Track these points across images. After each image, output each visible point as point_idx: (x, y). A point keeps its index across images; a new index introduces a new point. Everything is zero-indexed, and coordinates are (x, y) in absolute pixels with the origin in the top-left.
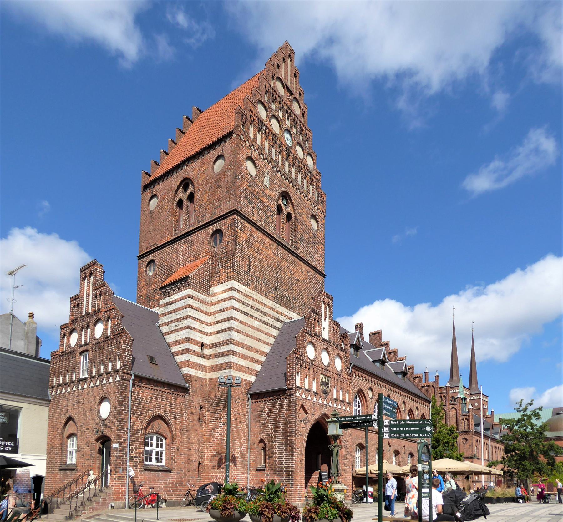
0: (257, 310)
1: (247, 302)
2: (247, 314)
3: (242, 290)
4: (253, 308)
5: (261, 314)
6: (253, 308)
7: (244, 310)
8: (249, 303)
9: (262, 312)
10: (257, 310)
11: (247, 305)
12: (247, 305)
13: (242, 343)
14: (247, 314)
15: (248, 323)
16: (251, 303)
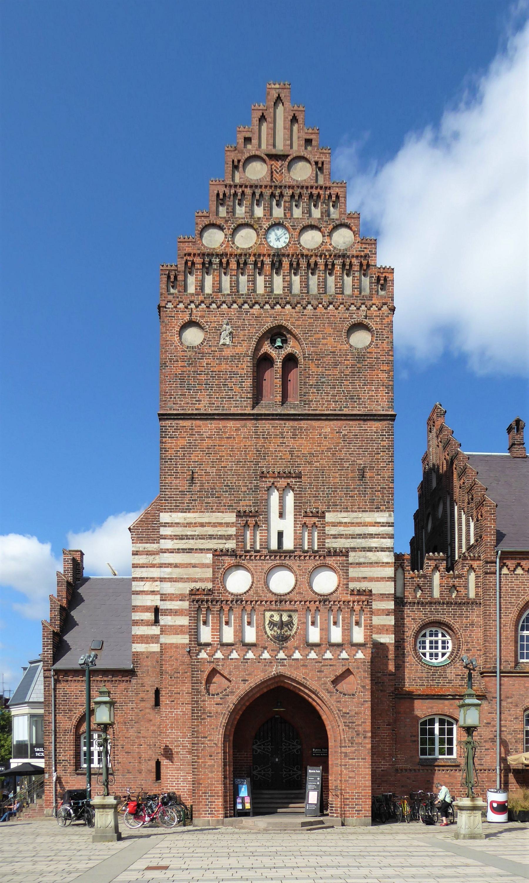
0: (211, 537)
1: (189, 533)
2: (190, 551)
3: (177, 521)
4: (202, 537)
5: (220, 541)
6: (202, 537)
7: (184, 547)
8: (193, 533)
9: (221, 537)
10: (211, 537)
11: (188, 537)
12: (188, 537)
13: (180, 594)
14: (190, 551)
15: (193, 562)
16: (199, 531)
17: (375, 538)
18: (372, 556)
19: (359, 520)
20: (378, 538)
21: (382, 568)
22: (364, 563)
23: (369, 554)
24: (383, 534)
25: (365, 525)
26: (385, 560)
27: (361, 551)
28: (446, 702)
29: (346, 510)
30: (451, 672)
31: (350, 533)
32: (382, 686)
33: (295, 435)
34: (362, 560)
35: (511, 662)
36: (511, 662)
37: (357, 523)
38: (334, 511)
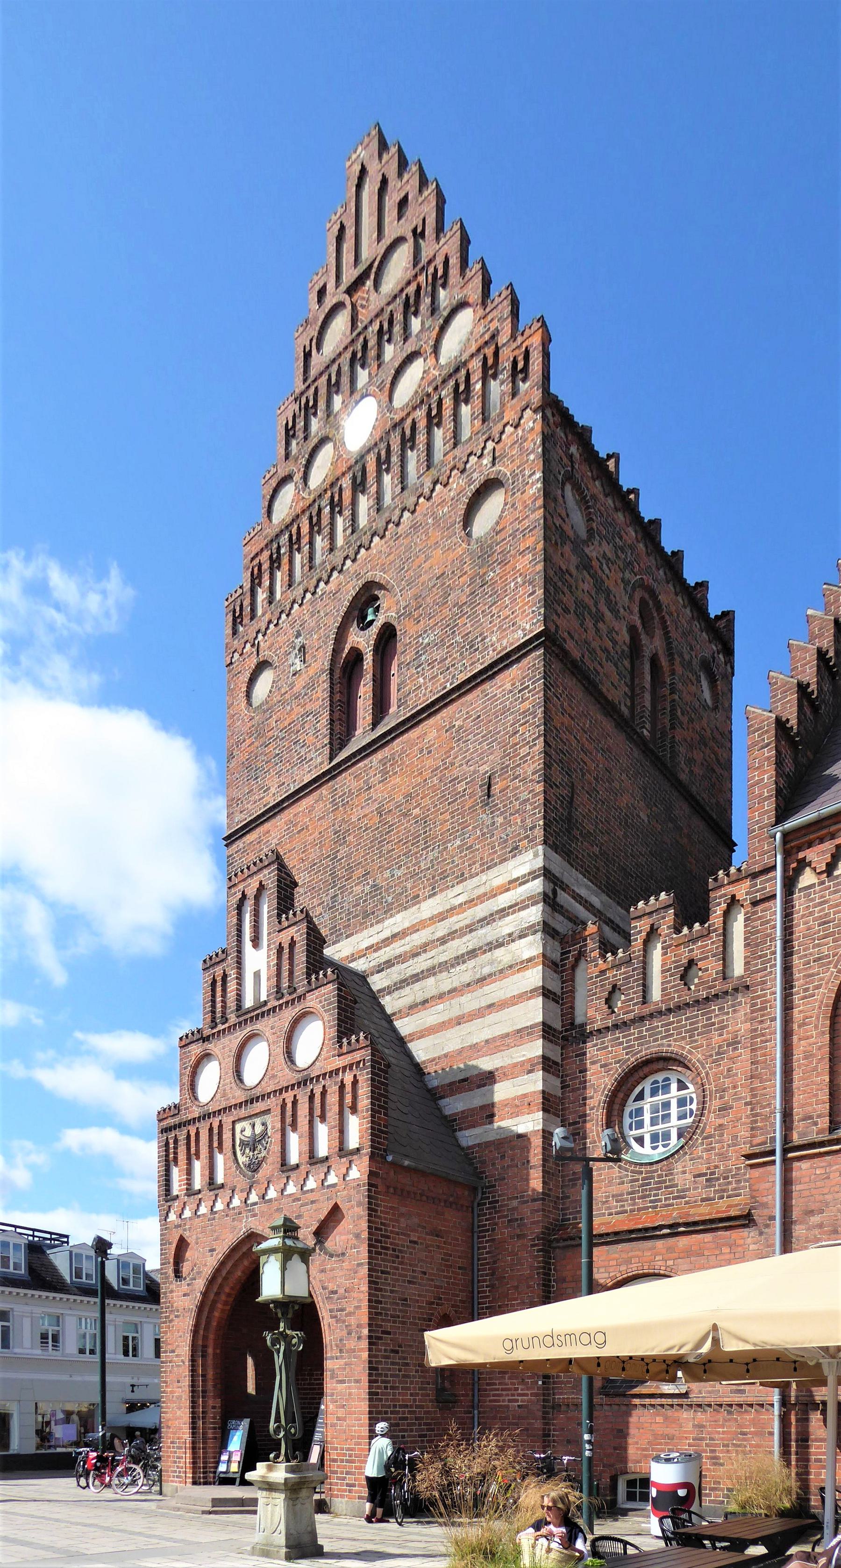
17: (508, 914)
18: (503, 956)
19: (482, 890)
20: (514, 912)
21: (521, 974)
22: (490, 975)
23: (499, 953)
24: (523, 901)
25: (493, 894)
26: (526, 955)
27: (485, 952)
28: (660, 1244)
29: (462, 878)
30: (683, 1174)
31: (467, 922)
32: (519, 1226)
33: (385, 772)
34: (486, 971)
35: (819, 1116)
36: (819, 1116)
37: (478, 897)
38: (442, 891)
